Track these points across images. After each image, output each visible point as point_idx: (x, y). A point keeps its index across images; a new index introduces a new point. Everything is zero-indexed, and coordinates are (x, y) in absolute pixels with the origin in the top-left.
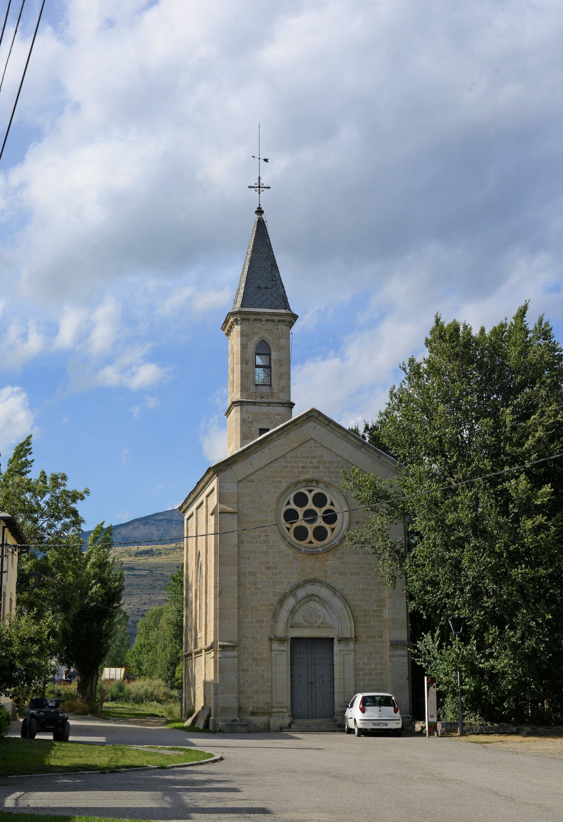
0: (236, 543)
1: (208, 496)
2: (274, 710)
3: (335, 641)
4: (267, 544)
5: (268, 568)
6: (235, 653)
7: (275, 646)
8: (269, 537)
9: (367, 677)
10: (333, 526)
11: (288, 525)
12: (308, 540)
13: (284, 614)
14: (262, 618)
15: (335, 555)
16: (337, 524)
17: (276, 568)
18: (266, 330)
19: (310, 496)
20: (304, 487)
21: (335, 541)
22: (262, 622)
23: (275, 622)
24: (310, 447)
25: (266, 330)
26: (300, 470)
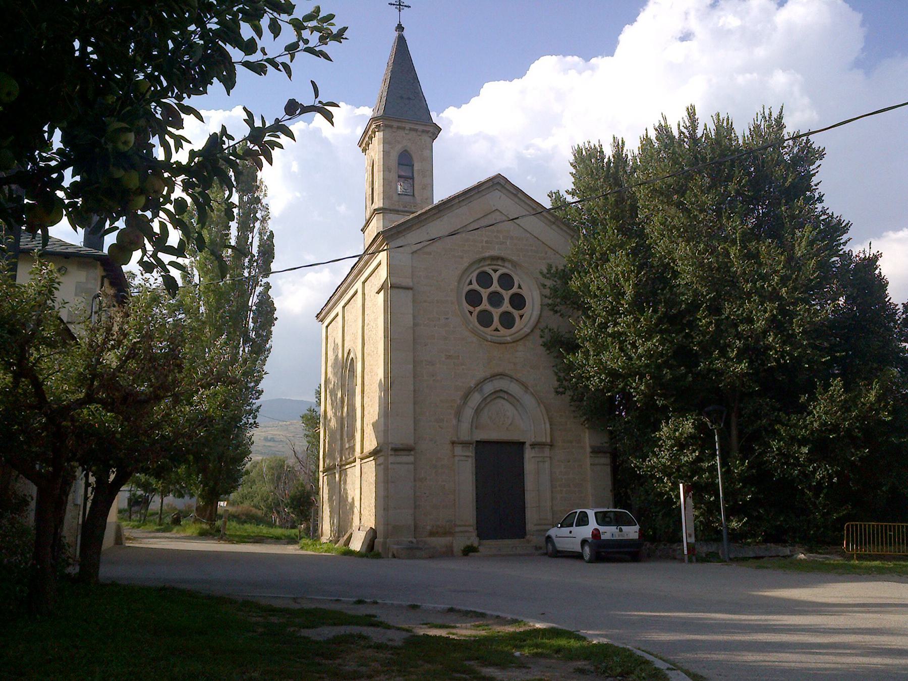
2: (457, 529)
3: (527, 445)
6: (411, 459)
7: (458, 450)
10: (521, 312)
11: (471, 309)
13: (468, 412)
19: (495, 277)
21: (525, 329)
26: (484, 244)
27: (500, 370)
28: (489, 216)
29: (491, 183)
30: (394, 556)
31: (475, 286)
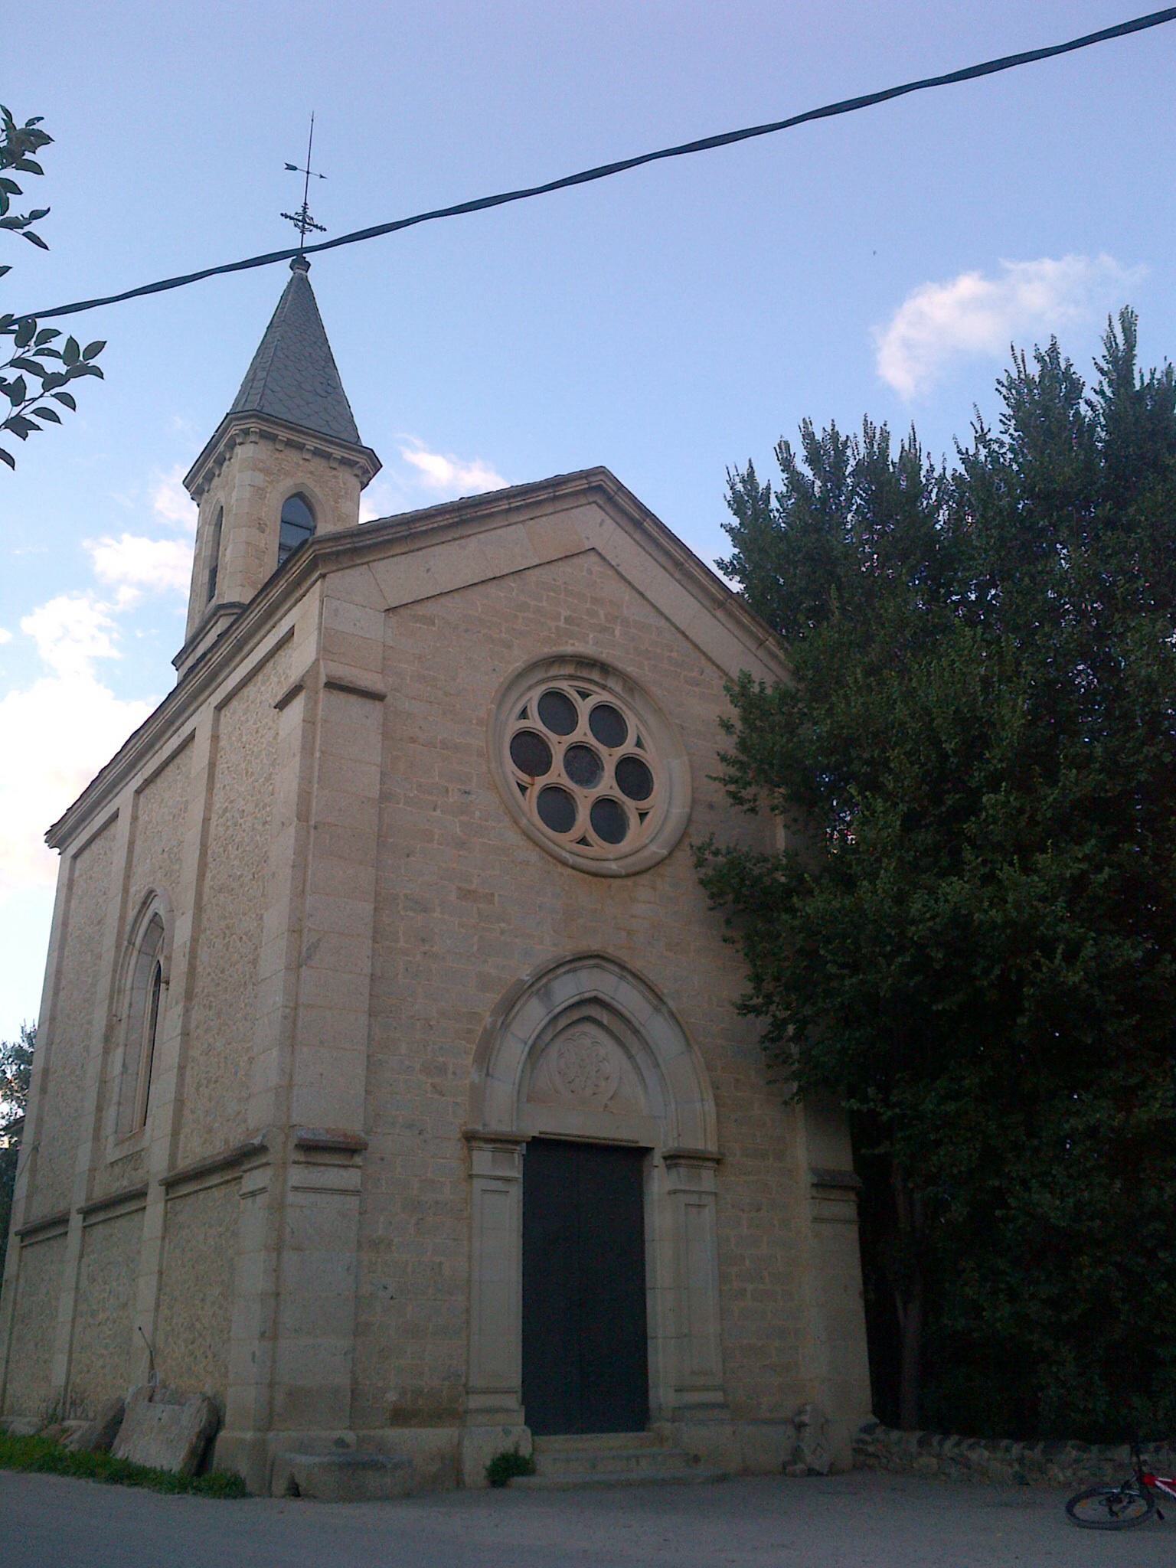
0: (375, 793)
1: (219, 708)
2: (474, 1402)
3: (657, 1159)
4: (464, 818)
5: (466, 894)
6: (349, 1178)
7: (483, 1160)
8: (473, 797)
9: (750, 1287)
10: (643, 804)
11: (525, 778)
12: (576, 832)
13: (512, 1053)
14: (441, 1059)
15: (654, 889)
16: (657, 799)
17: (489, 898)
18: (311, 473)
19: (584, 708)
20: (571, 677)
21: (653, 848)
22: (442, 1070)
23: (487, 1074)
24: (590, 572)
25: (311, 473)
26: (562, 624)
27: (595, 946)
28: (575, 560)
29: (583, 484)
30: (295, 1491)
31: (535, 723)
